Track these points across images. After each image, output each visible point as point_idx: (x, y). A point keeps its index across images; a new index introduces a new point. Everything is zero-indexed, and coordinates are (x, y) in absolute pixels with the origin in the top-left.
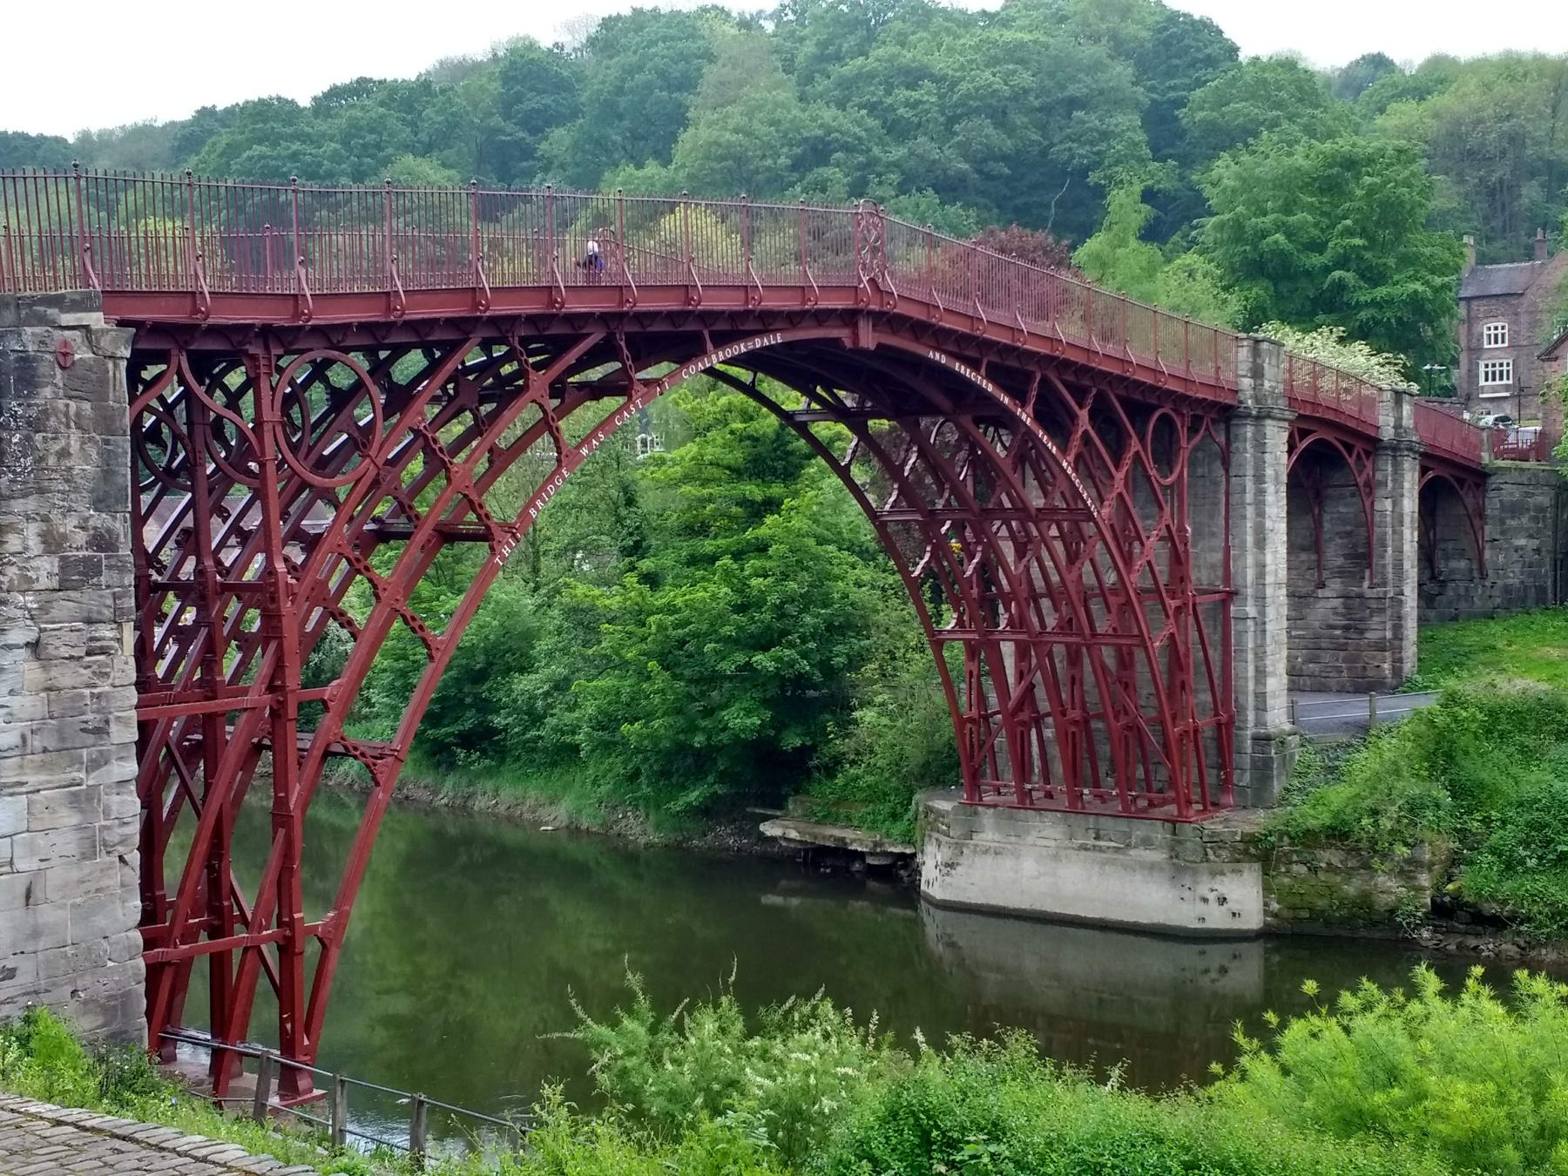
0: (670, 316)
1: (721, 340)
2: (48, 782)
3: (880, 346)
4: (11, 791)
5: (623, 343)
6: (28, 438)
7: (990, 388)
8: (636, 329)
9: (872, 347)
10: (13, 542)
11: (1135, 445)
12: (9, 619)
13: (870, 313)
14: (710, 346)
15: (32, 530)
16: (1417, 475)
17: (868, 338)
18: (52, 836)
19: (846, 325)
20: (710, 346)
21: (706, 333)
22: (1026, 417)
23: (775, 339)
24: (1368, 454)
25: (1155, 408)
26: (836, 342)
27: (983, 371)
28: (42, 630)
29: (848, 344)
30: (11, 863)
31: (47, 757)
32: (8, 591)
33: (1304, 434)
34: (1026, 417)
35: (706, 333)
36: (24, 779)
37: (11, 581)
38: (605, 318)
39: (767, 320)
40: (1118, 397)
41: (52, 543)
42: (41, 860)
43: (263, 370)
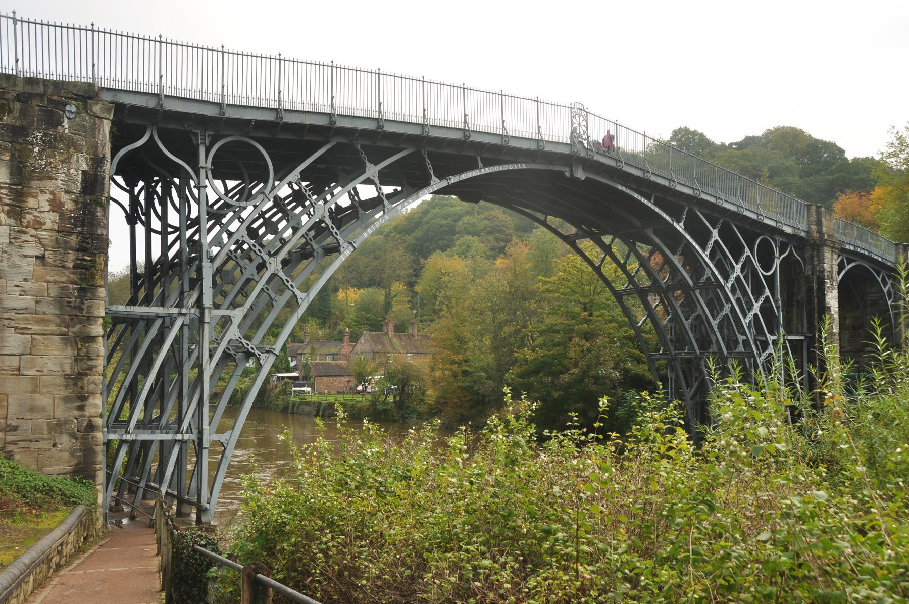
1: (487, 164)
2: (45, 330)
3: (587, 178)
4: (21, 331)
5: (426, 156)
7: (657, 210)
8: (433, 150)
9: (583, 178)
10: (31, 202)
11: (747, 252)
12: (26, 241)
14: (480, 164)
17: (580, 175)
18: (45, 359)
19: (566, 165)
20: (480, 164)
21: (479, 158)
23: (522, 166)
25: (761, 235)
26: (561, 173)
27: (652, 201)
28: (46, 250)
29: (567, 174)
30: (19, 370)
31: (42, 316)
32: (27, 227)
34: (680, 227)
35: (479, 158)
36: (29, 326)
37: (28, 222)
41: (56, 206)
42: (38, 371)
43: (200, 141)
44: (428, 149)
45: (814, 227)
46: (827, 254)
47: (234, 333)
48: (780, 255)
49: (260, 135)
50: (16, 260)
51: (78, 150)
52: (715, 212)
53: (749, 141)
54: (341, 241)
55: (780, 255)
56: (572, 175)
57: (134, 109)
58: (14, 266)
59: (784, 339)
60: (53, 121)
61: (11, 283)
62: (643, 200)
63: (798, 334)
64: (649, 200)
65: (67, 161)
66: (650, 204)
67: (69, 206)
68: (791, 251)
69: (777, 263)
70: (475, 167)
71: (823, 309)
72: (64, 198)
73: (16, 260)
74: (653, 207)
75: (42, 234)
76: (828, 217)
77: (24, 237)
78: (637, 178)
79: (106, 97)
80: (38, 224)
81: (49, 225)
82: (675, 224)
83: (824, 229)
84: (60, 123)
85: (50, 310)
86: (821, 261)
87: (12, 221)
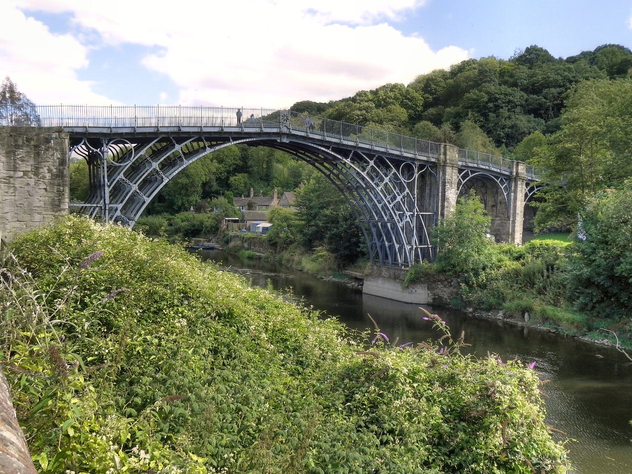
0: (215, 133)
1: (235, 140)
6: (44, 152)
7: (333, 153)
10: (41, 170)
13: (284, 134)
14: (231, 140)
15: (45, 169)
16: (524, 186)
17: (285, 140)
20: (231, 140)
24: (506, 180)
26: (276, 141)
29: (279, 141)
33: (472, 172)
39: (250, 135)
41: (50, 171)
45: (442, 156)
46: (449, 170)
47: (118, 213)
48: (418, 172)
50: (37, 190)
51: (57, 150)
52: (371, 154)
53: (584, 55)
54: (164, 177)
55: (418, 172)
57: (77, 133)
58: (36, 192)
59: (417, 215)
60: (47, 141)
61: (36, 198)
62: (324, 149)
64: (328, 149)
65: (53, 155)
66: (328, 151)
67: (55, 171)
69: (416, 175)
71: (444, 198)
72: (52, 168)
73: (37, 190)
74: (330, 152)
75: (46, 181)
76: (451, 151)
77: (39, 182)
78: (318, 140)
79: (66, 130)
80: (44, 177)
81: (48, 178)
82: (344, 159)
83: (448, 157)
84: (50, 142)
85: (49, 207)
86: (444, 174)
87: (35, 177)
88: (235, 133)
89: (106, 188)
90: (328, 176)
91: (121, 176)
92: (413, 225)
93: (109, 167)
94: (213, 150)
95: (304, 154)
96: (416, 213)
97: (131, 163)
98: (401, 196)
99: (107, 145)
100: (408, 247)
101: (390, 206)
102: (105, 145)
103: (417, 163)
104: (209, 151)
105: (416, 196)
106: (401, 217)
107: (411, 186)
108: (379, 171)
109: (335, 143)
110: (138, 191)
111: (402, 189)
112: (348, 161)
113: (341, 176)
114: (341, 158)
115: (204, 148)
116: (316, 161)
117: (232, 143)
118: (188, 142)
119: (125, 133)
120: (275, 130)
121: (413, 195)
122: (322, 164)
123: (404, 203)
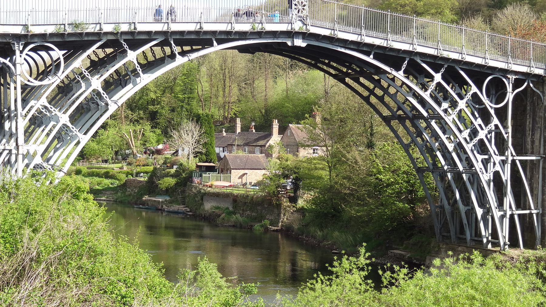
0: (190, 33)
1: (220, 42)
3: (308, 45)
5: (172, 42)
8: (178, 37)
14: (215, 43)
17: (299, 43)
19: (289, 37)
20: (215, 43)
21: (214, 39)
22: (400, 75)
29: (289, 44)
38: (157, 33)
40: (462, 69)
44: (175, 37)
48: (513, 90)
49: (55, 40)
54: (109, 102)
55: (513, 90)
56: (293, 44)
59: (513, 162)
63: (532, 154)
64: (368, 54)
68: (528, 84)
69: (510, 96)
70: (212, 45)
78: (353, 42)
82: (394, 73)
88: (221, 32)
89: (20, 119)
90: (366, 99)
91: (44, 101)
92: (506, 177)
93: (24, 87)
94: (185, 60)
95: (328, 65)
96: (510, 158)
97: (59, 81)
98: (486, 131)
99: (21, 52)
100: (497, 214)
101: (468, 147)
102: (18, 53)
103: (512, 77)
104: (180, 60)
105: (510, 130)
106: (485, 163)
107: (501, 114)
108: (448, 88)
109: (379, 47)
110: (69, 124)
111: (486, 118)
112: (400, 75)
113: (387, 99)
114: (390, 71)
115: (172, 57)
116: (347, 75)
117: (217, 47)
118: (146, 47)
119: (52, 35)
120: (284, 27)
121: (505, 127)
122: (357, 81)
123: (490, 142)
